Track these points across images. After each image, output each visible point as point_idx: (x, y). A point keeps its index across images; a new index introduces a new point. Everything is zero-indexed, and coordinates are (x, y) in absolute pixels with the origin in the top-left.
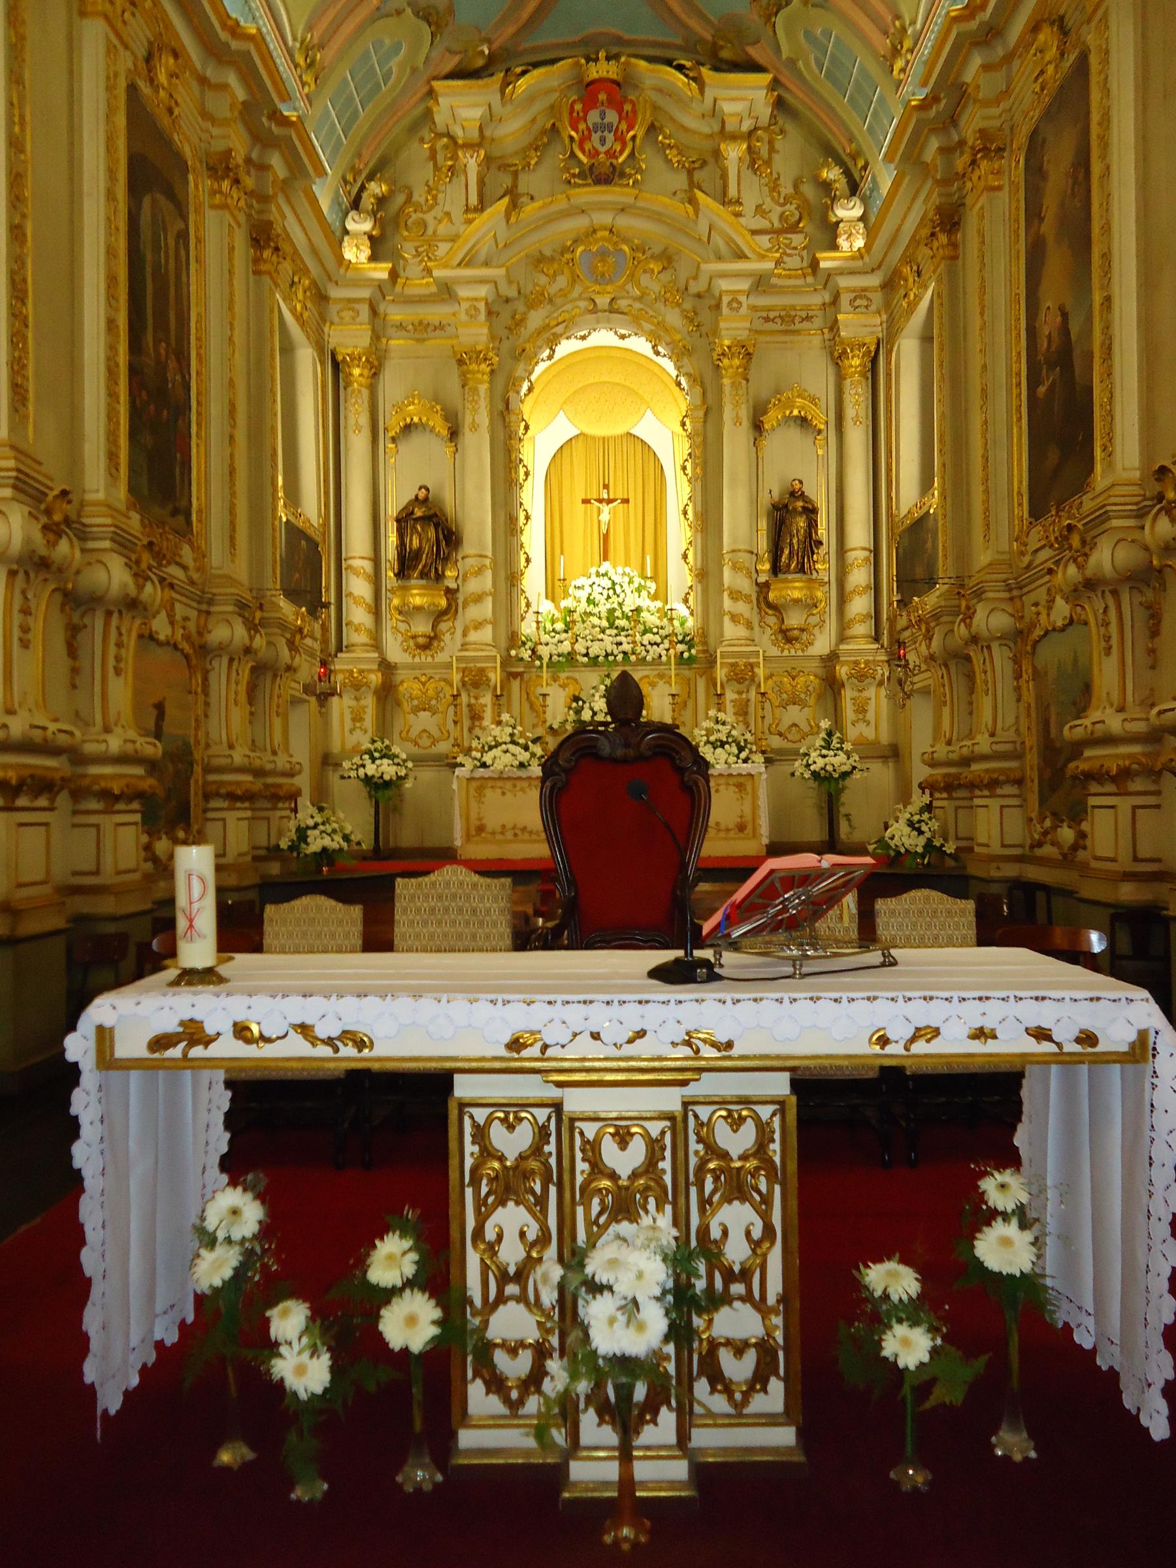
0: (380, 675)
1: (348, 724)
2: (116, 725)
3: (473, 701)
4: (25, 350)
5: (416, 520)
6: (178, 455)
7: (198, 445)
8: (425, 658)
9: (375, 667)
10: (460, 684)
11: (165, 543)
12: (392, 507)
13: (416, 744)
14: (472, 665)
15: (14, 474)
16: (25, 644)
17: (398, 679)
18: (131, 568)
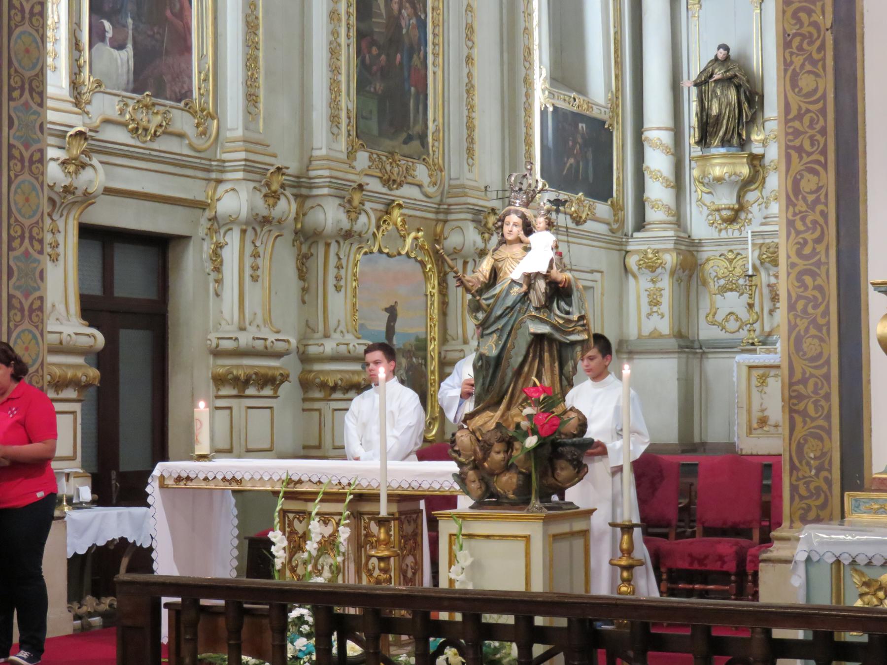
0: (675, 255)
1: (645, 308)
2: (335, 331)
3: (773, 280)
4: (257, 67)
5: (716, 81)
6: (413, 89)
7: (434, 73)
8: (733, 232)
9: (671, 246)
10: (758, 263)
11: (396, 170)
12: (694, 69)
13: (723, 328)
14: (767, 241)
15: (243, 163)
16: (255, 279)
17: (704, 256)
18: (344, 207)
